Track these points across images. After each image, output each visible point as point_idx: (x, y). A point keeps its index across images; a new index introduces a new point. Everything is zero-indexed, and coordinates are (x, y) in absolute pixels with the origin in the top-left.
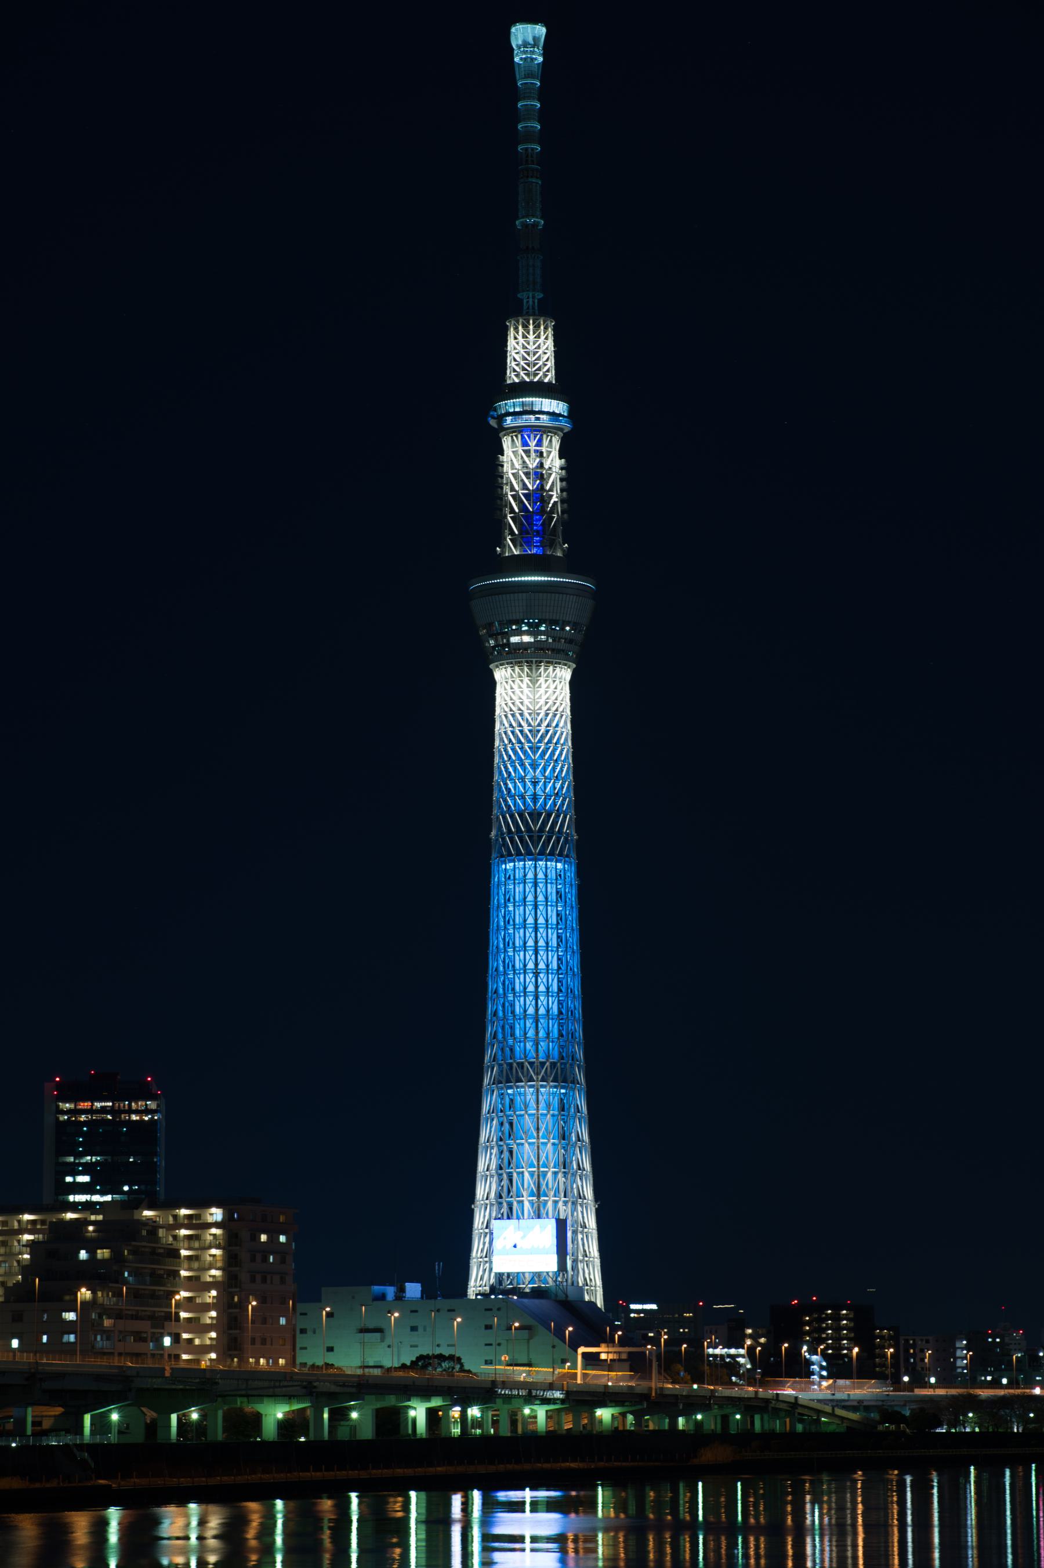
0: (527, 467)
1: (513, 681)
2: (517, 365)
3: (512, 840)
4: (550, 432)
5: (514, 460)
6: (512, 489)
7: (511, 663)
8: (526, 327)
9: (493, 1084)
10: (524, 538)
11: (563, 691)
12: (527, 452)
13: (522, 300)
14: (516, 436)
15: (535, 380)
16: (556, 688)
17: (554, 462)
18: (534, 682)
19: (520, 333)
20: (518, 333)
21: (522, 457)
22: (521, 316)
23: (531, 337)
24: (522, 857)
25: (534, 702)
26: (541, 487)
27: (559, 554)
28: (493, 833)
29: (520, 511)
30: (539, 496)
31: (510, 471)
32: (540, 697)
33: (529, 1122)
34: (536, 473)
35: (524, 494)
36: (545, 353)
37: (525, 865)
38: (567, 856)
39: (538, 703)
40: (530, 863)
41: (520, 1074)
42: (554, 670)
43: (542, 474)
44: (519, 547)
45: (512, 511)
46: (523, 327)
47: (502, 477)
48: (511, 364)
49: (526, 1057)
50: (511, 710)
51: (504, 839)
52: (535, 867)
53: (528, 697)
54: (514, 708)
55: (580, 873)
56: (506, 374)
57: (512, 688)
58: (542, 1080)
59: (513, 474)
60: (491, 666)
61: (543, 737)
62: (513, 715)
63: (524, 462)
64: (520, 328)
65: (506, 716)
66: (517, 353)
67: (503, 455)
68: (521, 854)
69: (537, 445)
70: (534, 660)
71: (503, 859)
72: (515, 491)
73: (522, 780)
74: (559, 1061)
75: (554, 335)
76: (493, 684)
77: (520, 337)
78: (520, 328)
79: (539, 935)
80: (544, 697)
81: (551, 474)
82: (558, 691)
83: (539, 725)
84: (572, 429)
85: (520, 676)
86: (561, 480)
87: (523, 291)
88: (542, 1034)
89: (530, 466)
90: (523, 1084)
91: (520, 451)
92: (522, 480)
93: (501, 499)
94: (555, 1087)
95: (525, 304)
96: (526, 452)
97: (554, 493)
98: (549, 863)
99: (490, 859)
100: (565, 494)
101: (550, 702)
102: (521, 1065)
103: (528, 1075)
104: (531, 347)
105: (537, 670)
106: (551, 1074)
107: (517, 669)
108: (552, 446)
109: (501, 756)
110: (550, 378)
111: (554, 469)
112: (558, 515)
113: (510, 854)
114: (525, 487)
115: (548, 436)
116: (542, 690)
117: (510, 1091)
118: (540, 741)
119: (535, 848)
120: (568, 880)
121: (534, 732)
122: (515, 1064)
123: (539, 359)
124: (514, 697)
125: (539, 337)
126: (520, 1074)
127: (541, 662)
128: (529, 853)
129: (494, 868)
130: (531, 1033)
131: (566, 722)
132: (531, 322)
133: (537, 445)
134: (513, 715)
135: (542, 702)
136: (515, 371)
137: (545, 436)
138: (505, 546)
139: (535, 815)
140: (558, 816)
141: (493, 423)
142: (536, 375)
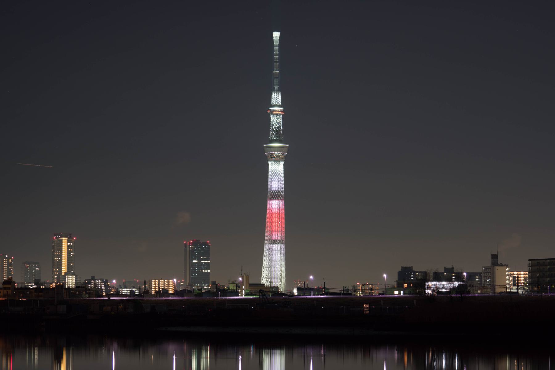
3: (274, 196)
5: (274, 120)
10: (276, 136)
12: (277, 119)
13: (274, 88)
35: (277, 127)
45: (274, 130)
51: (272, 196)
54: (275, 170)
76: (268, 165)
78: (276, 93)
91: (276, 118)
104: (278, 97)
114: (276, 125)
139: (279, 191)
142: (278, 103)
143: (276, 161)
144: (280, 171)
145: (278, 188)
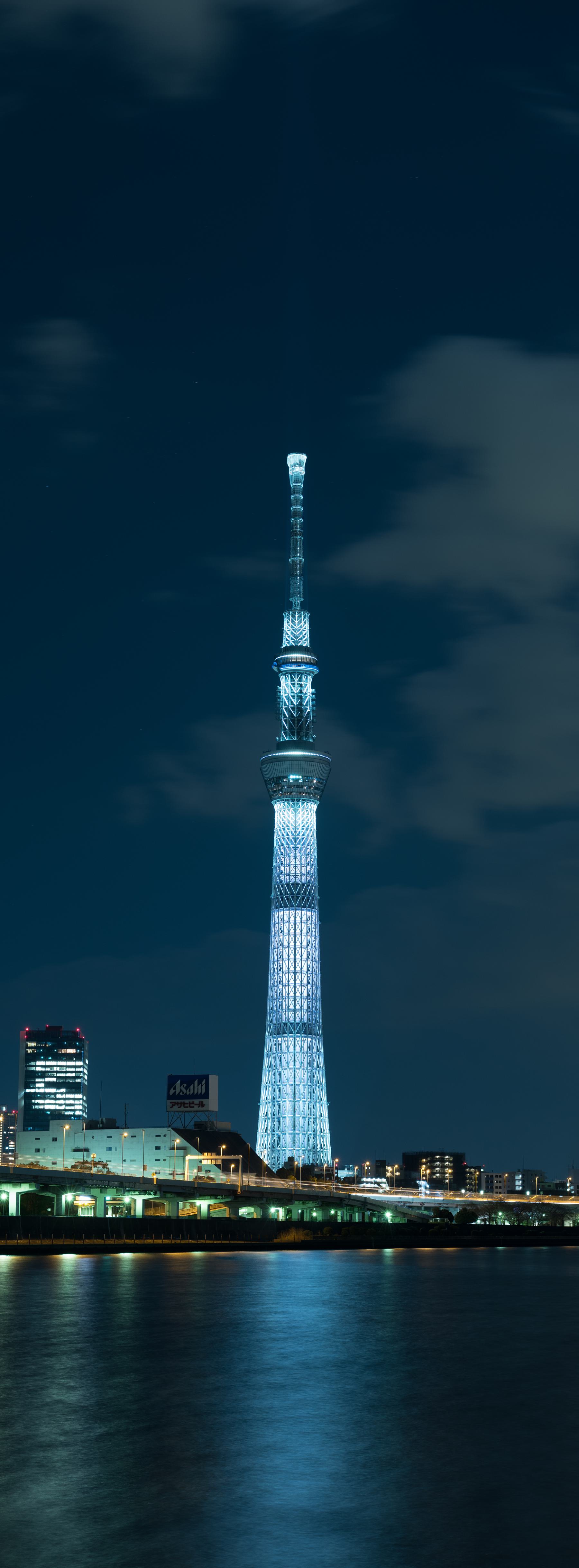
0: (293, 693)
1: (284, 810)
2: (289, 637)
4: (306, 673)
6: (285, 705)
7: (283, 800)
8: (293, 616)
9: (271, 1035)
11: (312, 816)
12: (294, 684)
14: (288, 676)
15: (299, 645)
16: (308, 814)
17: (309, 691)
18: (296, 811)
19: (291, 620)
20: (289, 620)
21: (291, 687)
22: (291, 610)
23: (297, 622)
24: (288, 908)
25: (296, 822)
26: (301, 704)
27: (311, 740)
28: (272, 895)
29: (289, 717)
30: (300, 708)
31: (284, 695)
32: (299, 819)
33: (289, 1057)
34: (298, 696)
35: (292, 708)
36: (304, 631)
37: (289, 912)
38: (313, 908)
39: (298, 822)
40: (292, 911)
41: (285, 1030)
42: (307, 804)
43: (301, 696)
44: (288, 737)
45: (285, 717)
46: (292, 616)
47: (280, 698)
48: (285, 636)
49: (288, 1020)
50: (283, 826)
51: (278, 898)
52: (295, 914)
53: (292, 819)
54: (285, 826)
55: (321, 918)
56: (283, 642)
57: (283, 814)
58: (298, 1033)
59: (286, 697)
60: (272, 802)
61: (300, 841)
62: (284, 829)
63: (292, 690)
64: (291, 616)
65: (280, 830)
66: (289, 630)
67: (280, 686)
68: (287, 907)
69: (298, 681)
70: (296, 798)
71: (277, 909)
72: (287, 706)
73: (289, 865)
74: (307, 1022)
75: (310, 621)
77: (290, 622)
78: (291, 616)
79: (297, 952)
80: (301, 819)
81: (306, 697)
82: (309, 816)
83: (298, 835)
84: (319, 673)
85: (288, 808)
86: (313, 700)
87: (292, 597)
88: (298, 1007)
89: (295, 692)
90: (287, 1035)
91: (289, 683)
92: (291, 700)
93: (279, 711)
94: (305, 1037)
95: (293, 604)
96: (293, 684)
97: (309, 707)
98: (303, 912)
99: (271, 909)
100: (314, 708)
101: (305, 822)
102: (286, 1024)
103: (289, 1029)
105: (298, 804)
106: (303, 1029)
107: (286, 803)
108: (308, 682)
109: (277, 852)
110: (307, 644)
111: (308, 694)
112: (310, 719)
113: (281, 907)
115: (305, 676)
116: (300, 815)
117: (280, 1039)
118: (299, 843)
119: (295, 903)
120: (314, 933)
121: (295, 839)
122: (282, 1024)
123: (300, 633)
124: (284, 819)
125: (301, 622)
126: (285, 1030)
127: (299, 800)
128: (292, 906)
129: (273, 914)
130: (292, 1007)
131: (313, 834)
132: (296, 613)
133: (298, 681)
134: (284, 829)
135: (300, 822)
136: (287, 640)
137: (303, 676)
138: (281, 736)
139: (295, 885)
140: (308, 886)
141: (275, 669)
142: (299, 642)
143: (288, 801)
144: (300, 827)
145: (292, 877)
